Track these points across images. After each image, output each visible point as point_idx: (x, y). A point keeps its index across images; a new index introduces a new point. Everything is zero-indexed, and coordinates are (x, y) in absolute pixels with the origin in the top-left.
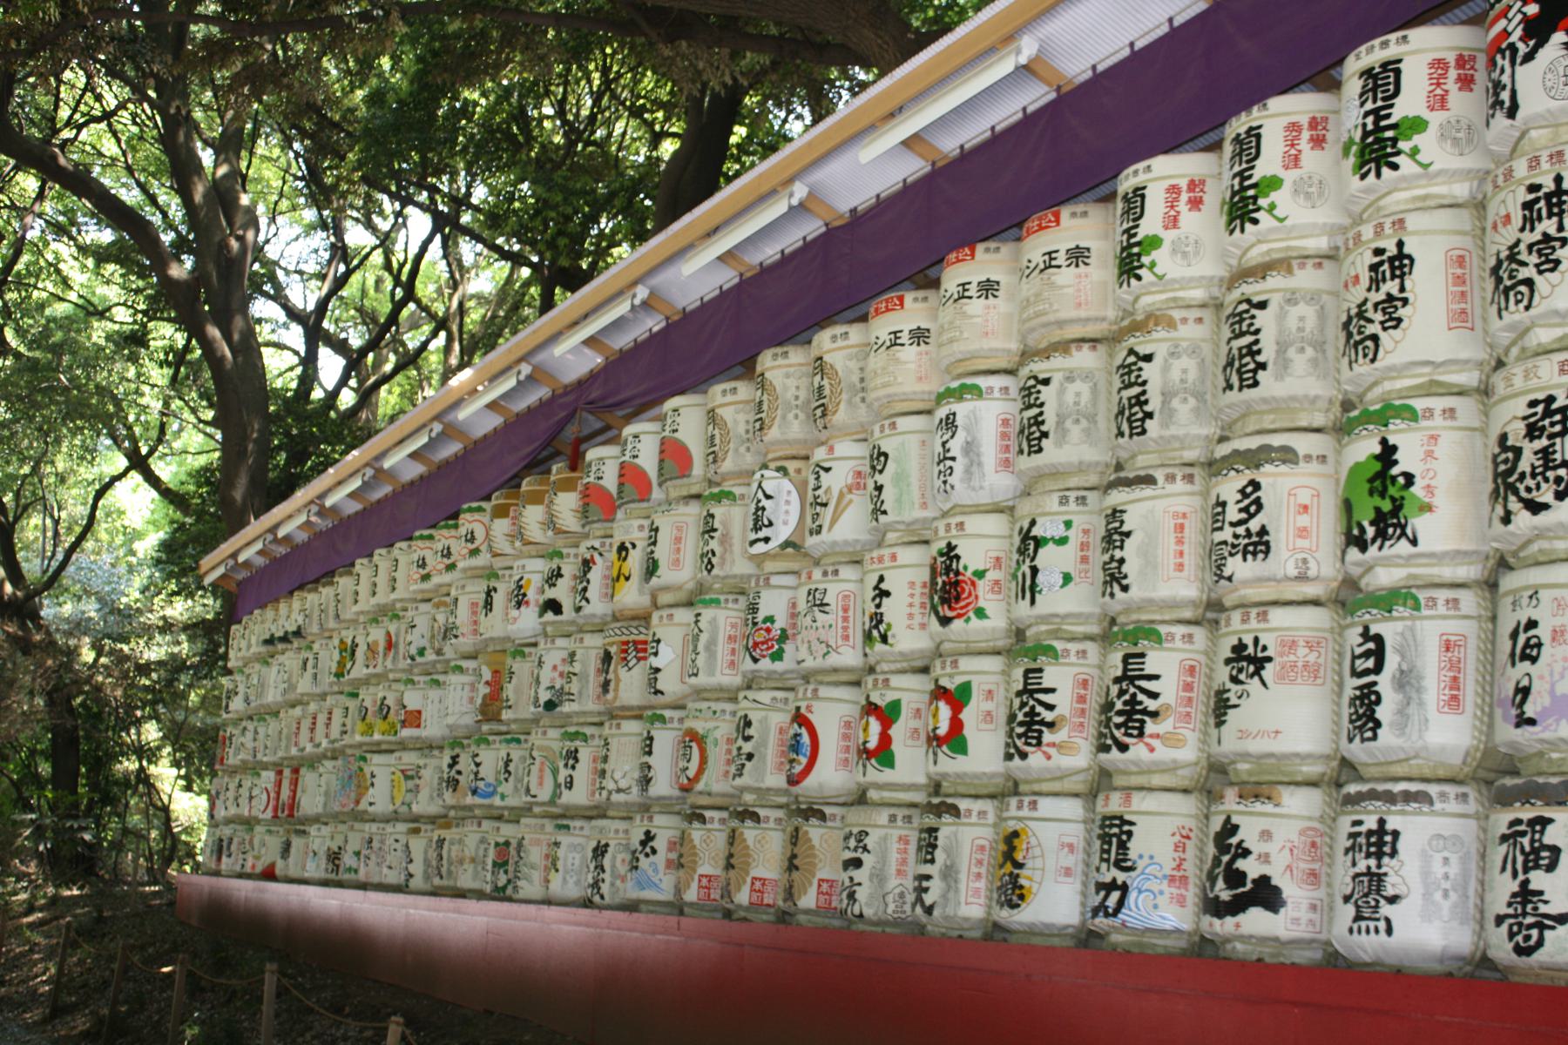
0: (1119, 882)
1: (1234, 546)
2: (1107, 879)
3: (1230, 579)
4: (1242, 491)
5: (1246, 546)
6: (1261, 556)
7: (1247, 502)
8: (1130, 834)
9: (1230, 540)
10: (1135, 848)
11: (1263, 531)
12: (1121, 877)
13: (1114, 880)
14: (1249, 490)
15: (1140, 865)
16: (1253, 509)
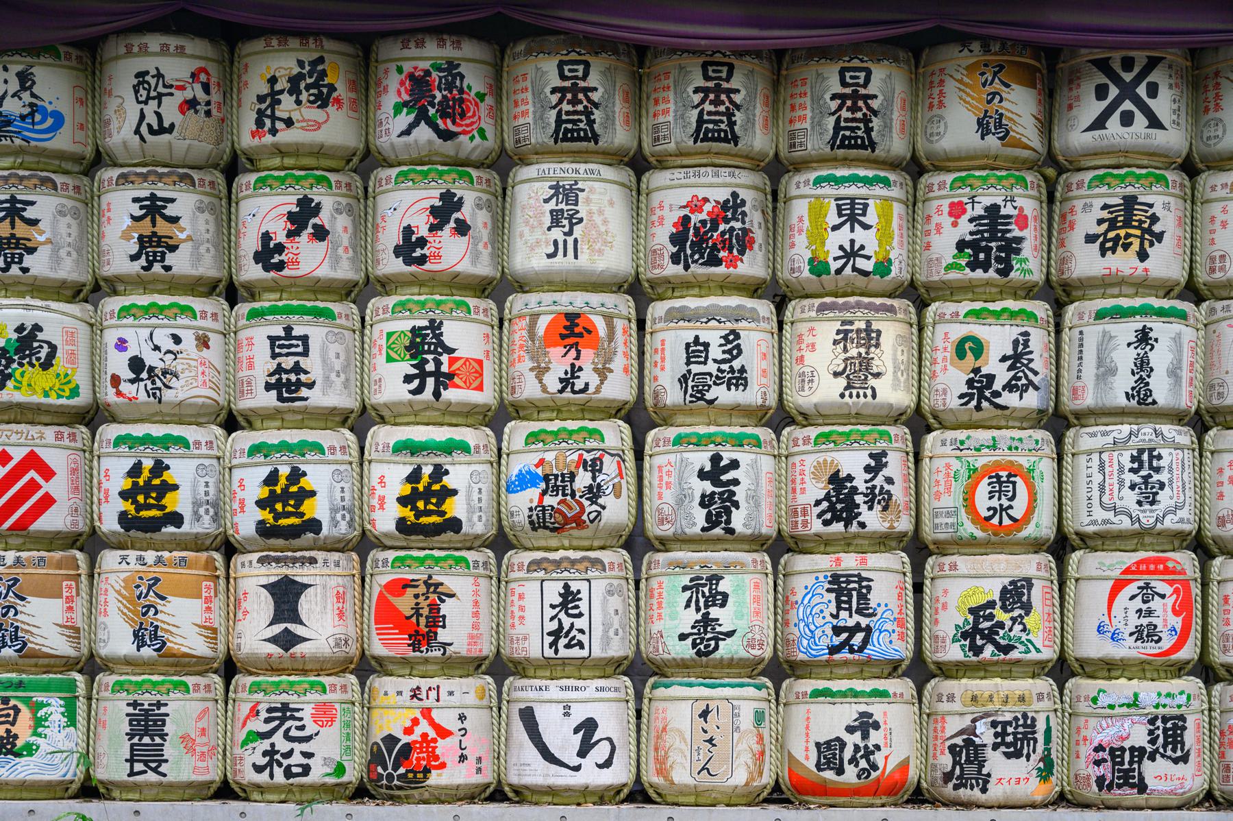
0: (863, 626)
1: (717, 377)
2: (851, 623)
3: (711, 402)
4: (725, 337)
5: (730, 379)
6: (741, 388)
7: (729, 346)
8: (869, 588)
9: (715, 373)
10: (874, 599)
11: (743, 370)
12: (864, 622)
13: (858, 624)
14: (731, 337)
15: (880, 611)
16: (735, 352)
